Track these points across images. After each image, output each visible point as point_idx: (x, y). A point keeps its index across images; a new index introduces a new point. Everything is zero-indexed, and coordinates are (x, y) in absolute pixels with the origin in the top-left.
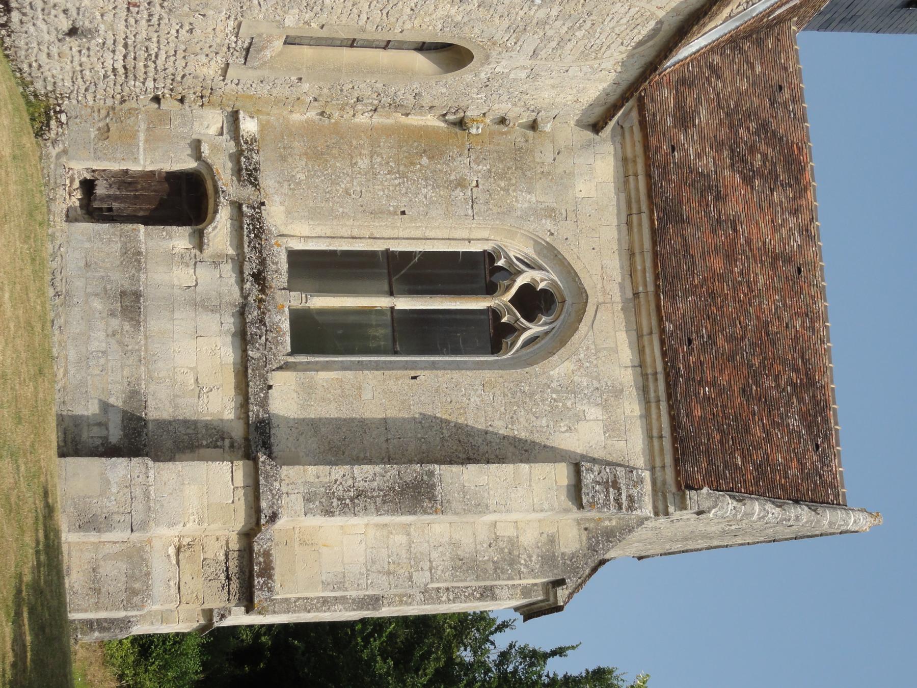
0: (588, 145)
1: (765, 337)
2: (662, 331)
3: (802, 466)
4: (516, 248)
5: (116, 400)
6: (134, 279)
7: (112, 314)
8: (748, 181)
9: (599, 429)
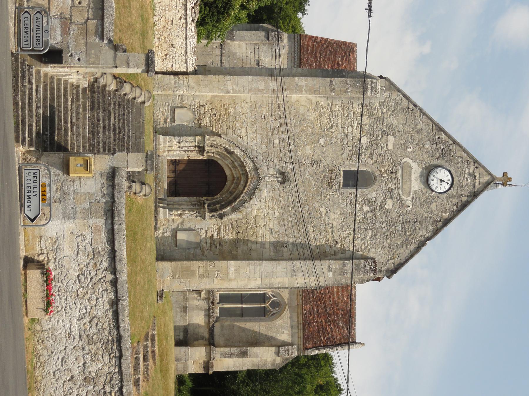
2: (303, 314)
6: (186, 304)
7: (181, 312)
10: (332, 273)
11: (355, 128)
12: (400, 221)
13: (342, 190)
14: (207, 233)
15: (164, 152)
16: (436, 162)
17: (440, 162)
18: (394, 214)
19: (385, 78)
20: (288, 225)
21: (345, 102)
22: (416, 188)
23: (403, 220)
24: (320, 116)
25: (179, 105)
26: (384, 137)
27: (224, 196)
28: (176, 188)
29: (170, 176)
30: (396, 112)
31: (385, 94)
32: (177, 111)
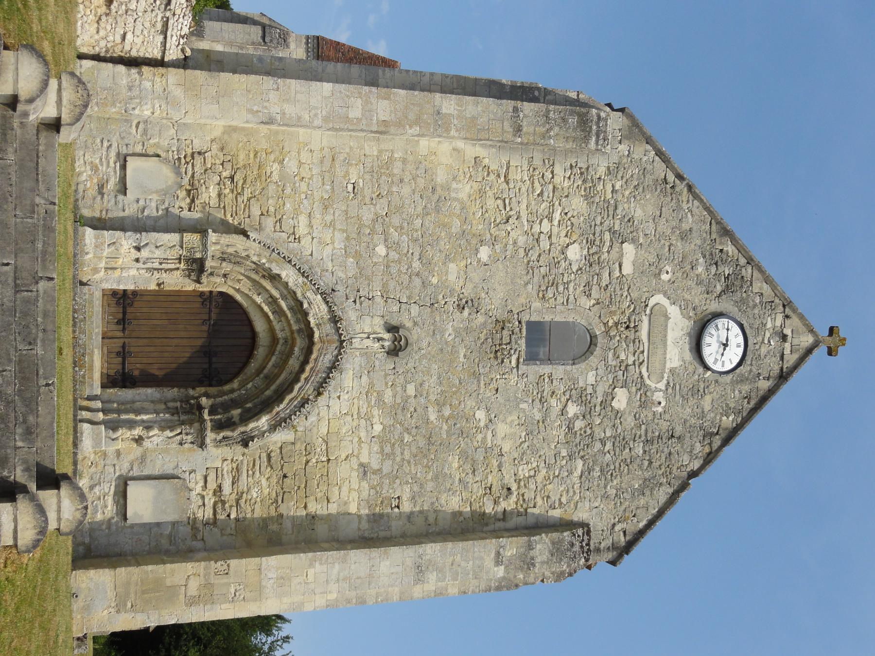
10: (502, 567)
11: (556, 223)
12: (640, 437)
13: (523, 368)
14: (206, 482)
15: (96, 270)
17: (725, 305)
18: (630, 421)
19: (622, 110)
20: (402, 454)
21: (537, 162)
23: (646, 434)
24: (482, 193)
25: (139, 149)
26: (616, 245)
27: (250, 385)
28: (123, 364)
29: (110, 334)
30: (641, 189)
31: (621, 147)
32: (133, 164)
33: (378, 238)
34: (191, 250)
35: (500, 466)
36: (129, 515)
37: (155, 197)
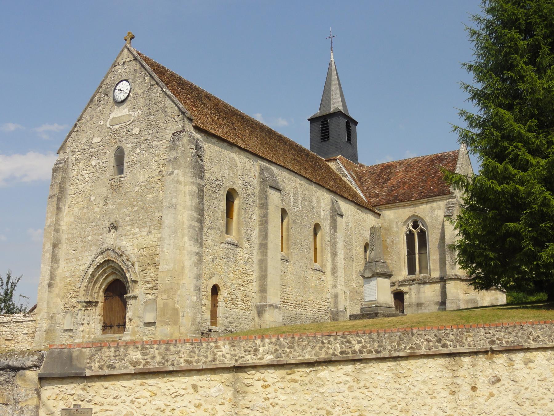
0: (383, 216)
1: (422, 173)
3: (450, 162)
4: (405, 230)
5: (438, 307)
6: (414, 305)
8: (390, 179)
9: (439, 211)
16: (111, 99)
18: (143, 125)
22: (127, 110)
33: (86, 239)
34: (83, 306)
35: (153, 177)
36: (153, 321)
37: (73, 319)
